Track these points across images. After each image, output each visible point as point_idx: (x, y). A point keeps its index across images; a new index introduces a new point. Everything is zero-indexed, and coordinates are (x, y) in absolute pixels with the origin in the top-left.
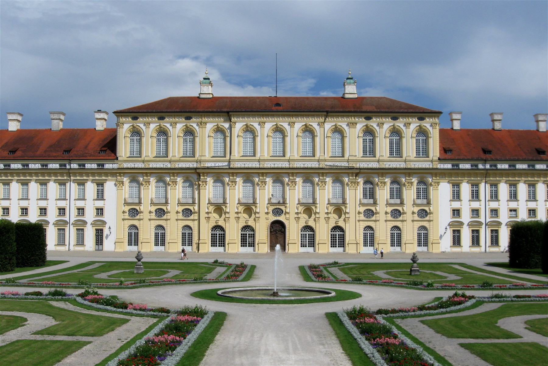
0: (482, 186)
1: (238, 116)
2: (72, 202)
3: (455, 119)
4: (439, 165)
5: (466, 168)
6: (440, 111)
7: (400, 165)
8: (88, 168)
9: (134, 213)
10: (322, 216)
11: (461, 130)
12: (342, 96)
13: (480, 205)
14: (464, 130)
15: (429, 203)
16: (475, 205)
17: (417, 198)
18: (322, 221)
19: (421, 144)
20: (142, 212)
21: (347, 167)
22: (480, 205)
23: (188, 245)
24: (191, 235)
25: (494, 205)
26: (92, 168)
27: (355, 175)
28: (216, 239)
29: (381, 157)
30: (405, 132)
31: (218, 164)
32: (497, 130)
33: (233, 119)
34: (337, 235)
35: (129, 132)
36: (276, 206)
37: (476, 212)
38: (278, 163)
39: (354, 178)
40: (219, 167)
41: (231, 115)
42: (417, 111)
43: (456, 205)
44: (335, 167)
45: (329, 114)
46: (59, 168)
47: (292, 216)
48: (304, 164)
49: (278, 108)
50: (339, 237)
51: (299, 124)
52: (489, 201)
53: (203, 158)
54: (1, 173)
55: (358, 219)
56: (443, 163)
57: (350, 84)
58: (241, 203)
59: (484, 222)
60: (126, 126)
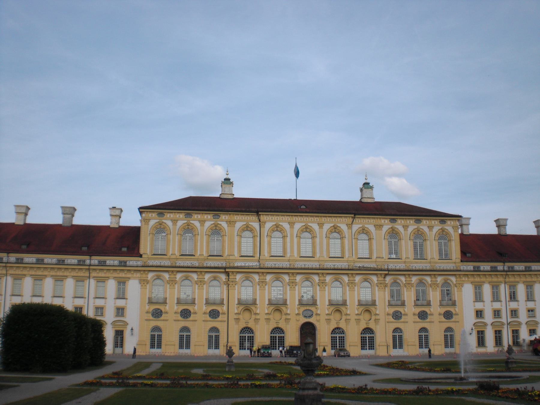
0: (502, 287)
2: (91, 300)
6: (460, 215)
9: (157, 314)
10: (353, 317)
13: (501, 306)
15: (454, 304)
16: (497, 305)
18: (353, 322)
19: (393, 246)
20: (406, 315)
22: (501, 306)
23: (215, 348)
24: (217, 337)
25: (513, 305)
27: (383, 276)
30: (428, 235)
31: (240, 264)
34: (338, 337)
35: (210, 230)
37: (497, 313)
39: (383, 279)
45: (356, 216)
46: (473, 270)
47: (323, 318)
50: (369, 340)
53: (231, 257)
55: (387, 320)
59: (505, 322)
60: (152, 223)
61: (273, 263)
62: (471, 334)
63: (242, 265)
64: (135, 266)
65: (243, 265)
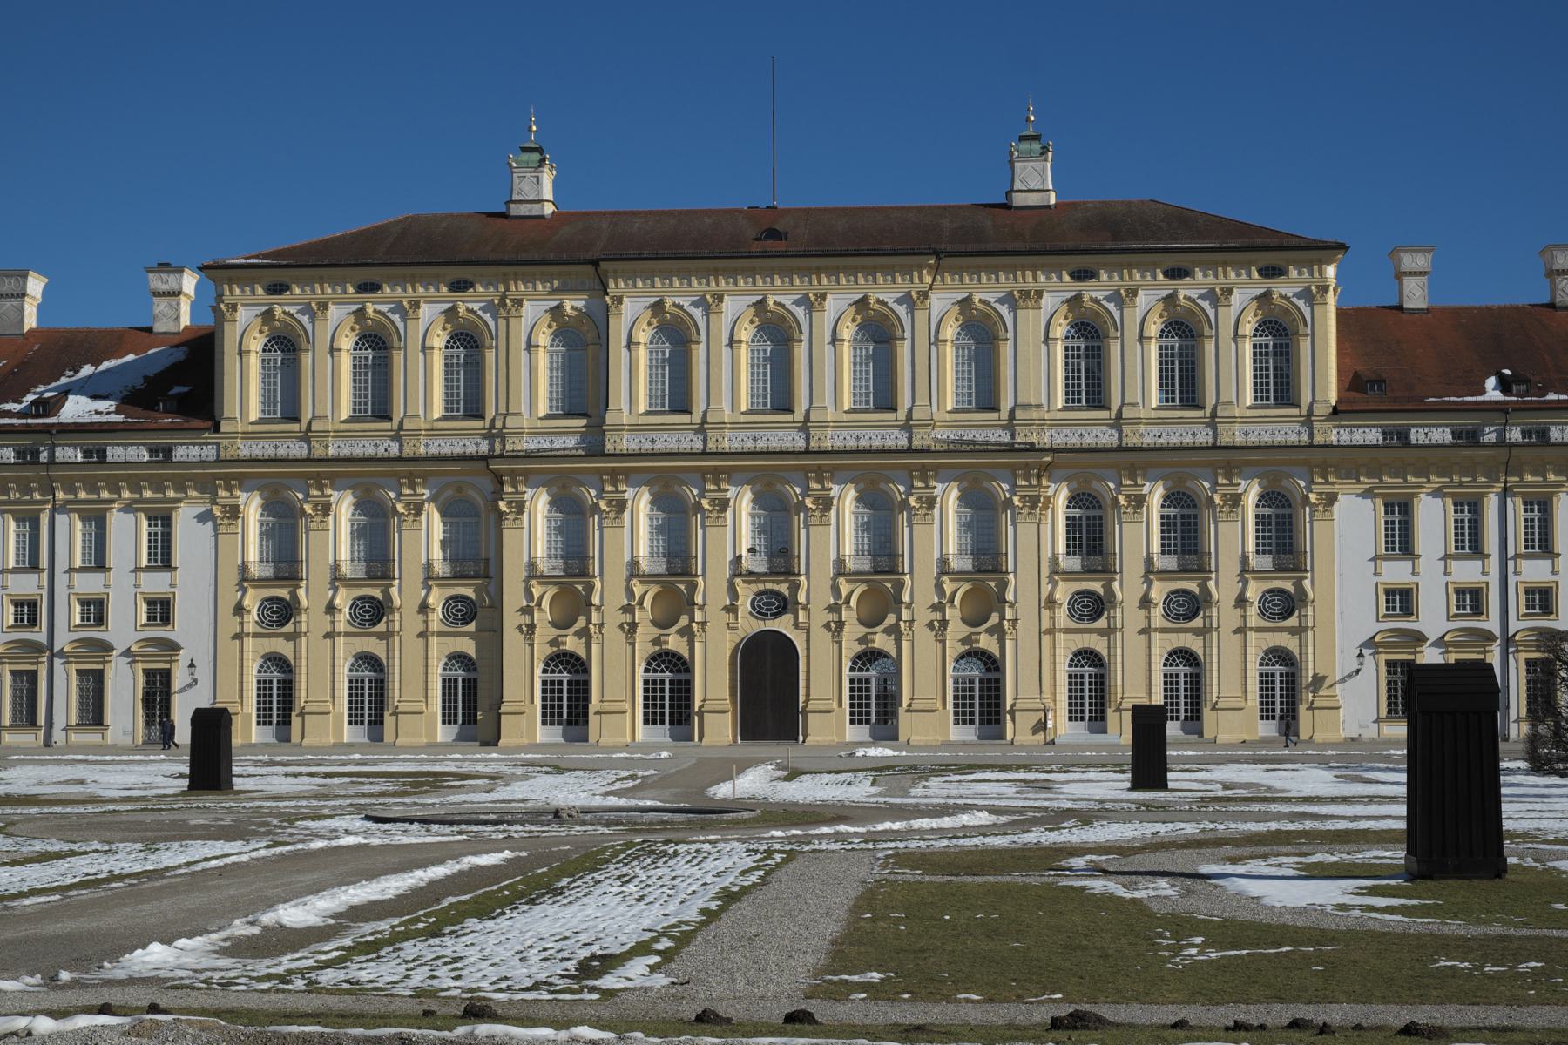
1: (630, 277)
3: (1410, 274)
4: (1335, 431)
5: (1434, 442)
7: (1194, 434)
8: (116, 459)
11: (1428, 310)
14: (1443, 310)
16: (1467, 572)
26: (129, 459)
28: (560, 699)
33: (612, 284)
36: (764, 582)
37: (1471, 599)
38: (768, 433)
39: (1035, 482)
40: (567, 452)
41: (606, 271)
42: (1258, 242)
43: (1397, 572)
47: (820, 617)
48: (858, 438)
49: (770, 245)
51: (838, 303)
52: (1516, 556)
56: (1347, 427)
58: (644, 576)
59: (1497, 632)
62: (1358, 671)
63: (541, 446)
64: (194, 460)
65: (545, 446)
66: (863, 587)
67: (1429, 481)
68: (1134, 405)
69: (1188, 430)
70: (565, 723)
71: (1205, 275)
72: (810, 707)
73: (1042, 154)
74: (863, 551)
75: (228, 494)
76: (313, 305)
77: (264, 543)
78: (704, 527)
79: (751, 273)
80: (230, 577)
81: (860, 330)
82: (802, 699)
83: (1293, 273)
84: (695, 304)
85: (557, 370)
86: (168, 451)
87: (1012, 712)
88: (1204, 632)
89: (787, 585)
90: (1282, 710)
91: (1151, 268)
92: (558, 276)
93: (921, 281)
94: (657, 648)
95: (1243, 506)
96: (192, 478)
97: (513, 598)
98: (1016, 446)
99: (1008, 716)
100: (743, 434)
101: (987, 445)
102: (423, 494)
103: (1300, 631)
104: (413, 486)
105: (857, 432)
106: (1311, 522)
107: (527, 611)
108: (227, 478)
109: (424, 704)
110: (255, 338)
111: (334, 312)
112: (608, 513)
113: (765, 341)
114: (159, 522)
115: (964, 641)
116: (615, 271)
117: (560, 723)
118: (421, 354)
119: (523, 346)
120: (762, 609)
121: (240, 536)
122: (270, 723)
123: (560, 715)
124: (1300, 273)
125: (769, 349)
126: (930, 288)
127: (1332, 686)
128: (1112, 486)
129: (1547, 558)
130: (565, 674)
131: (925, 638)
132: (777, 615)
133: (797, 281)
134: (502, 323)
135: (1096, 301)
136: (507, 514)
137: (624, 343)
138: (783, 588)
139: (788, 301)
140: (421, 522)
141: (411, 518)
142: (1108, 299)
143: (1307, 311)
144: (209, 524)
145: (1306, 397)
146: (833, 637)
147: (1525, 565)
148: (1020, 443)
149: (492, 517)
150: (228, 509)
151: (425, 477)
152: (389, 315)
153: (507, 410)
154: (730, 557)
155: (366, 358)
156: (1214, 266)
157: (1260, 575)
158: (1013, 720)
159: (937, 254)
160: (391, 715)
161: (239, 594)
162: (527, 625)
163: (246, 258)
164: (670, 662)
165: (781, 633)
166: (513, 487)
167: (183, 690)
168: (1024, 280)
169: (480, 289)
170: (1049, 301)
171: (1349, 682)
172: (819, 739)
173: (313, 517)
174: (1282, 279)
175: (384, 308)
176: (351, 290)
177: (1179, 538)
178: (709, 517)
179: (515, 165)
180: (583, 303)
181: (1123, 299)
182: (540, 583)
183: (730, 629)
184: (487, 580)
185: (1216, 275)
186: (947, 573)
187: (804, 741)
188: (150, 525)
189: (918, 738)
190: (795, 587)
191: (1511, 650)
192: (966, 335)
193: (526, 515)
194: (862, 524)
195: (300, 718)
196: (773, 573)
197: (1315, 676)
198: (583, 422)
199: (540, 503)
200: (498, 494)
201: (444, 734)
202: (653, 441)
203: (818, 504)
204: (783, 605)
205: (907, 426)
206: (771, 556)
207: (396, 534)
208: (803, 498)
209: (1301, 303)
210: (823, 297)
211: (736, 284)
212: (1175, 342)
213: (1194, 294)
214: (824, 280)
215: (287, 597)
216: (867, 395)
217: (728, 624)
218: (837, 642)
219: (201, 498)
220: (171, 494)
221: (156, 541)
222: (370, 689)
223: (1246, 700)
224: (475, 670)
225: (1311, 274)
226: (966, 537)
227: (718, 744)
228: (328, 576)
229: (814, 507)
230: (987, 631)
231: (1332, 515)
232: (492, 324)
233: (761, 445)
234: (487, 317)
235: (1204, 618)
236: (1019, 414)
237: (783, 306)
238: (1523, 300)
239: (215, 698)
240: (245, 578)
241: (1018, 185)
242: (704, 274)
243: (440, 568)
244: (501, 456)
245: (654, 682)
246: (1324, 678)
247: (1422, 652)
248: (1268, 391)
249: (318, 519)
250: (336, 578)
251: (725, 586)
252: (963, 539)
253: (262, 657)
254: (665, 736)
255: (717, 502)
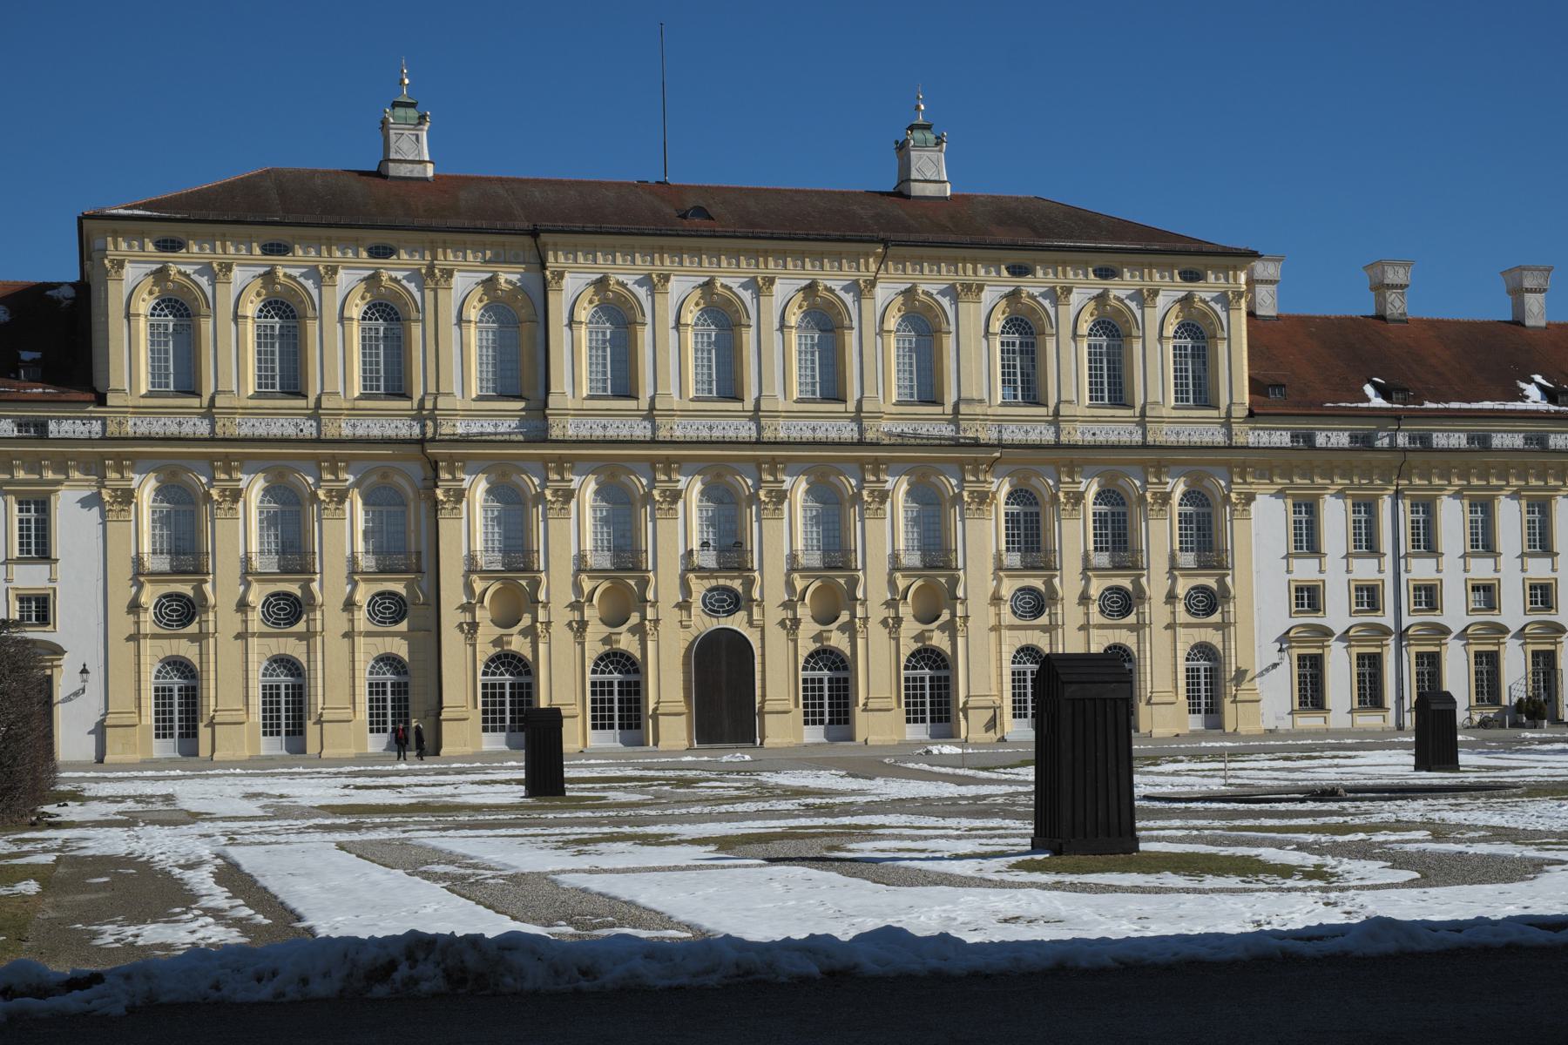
1: (572, 251)
11: (1278, 318)
12: (890, 187)
13: (1380, 571)
14: (1289, 318)
16: (1366, 570)
17: (1096, 549)
21: (951, 439)
25: (1421, 570)
29: (1066, 405)
32: (1395, 321)
33: (551, 258)
36: (717, 578)
37: (1368, 596)
38: (724, 422)
41: (545, 245)
43: (1306, 570)
44: (918, 441)
47: (774, 614)
48: (814, 429)
52: (1407, 555)
54: (11, 456)
56: (1267, 429)
57: (924, 145)
61: (584, 421)
62: (1275, 665)
64: (82, 437)
65: (489, 430)
66: (817, 583)
67: (1450, 484)
68: (1070, 402)
69: (1118, 429)
70: (507, 729)
71: (1132, 276)
72: (767, 708)
73: (937, 144)
74: (812, 546)
75: (118, 476)
76: (215, 265)
77: (157, 532)
78: (654, 520)
79: (697, 252)
80: (122, 572)
81: (805, 317)
82: (758, 699)
83: (1211, 277)
84: (639, 283)
85: (487, 348)
86: (41, 427)
87: (965, 710)
88: (1137, 628)
89: (740, 581)
90: (1206, 704)
91: (1084, 266)
92: (491, 246)
93: (867, 269)
94: (607, 648)
95: (1085, 504)
96: (76, 457)
97: (452, 594)
98: (962, 441)
99: (961, 714)
100: (697, 422)
101: (940, 439)
102: (347, 480)
103: (1223, 626)
104: (334, 471)
105: (813, 423)
106: (1231, 520)
107: (465, 608)
108: (119, 459)
109: (351, 711)
110: (143, 300)
111: (239, 275)
112: (553, 503)
113: (708, 325)
114: (33, 507)
115: (917, 638)
116: (555, 245)
117: (502, 729)
118: (338, 325)
119: (454, 321)
120: (714, 606)
121: (133, 523)
122: (172, 735)
123: (503, 720)
124: (1217, 278)
125: (713, 334)
126: (876, 278)
127: (1253, 679)
128: (1051, 482)
129: (1375, 558)
130: (507, 676)
131: (878, 634)
132: (730, 613)
133: (743, 263)
134: (429, 295)
135: (1032, 297)
136: (445, 503)
137: (565, 321)
138: (737, 585)
139: (734, 283)
140: (344, 511)
141: (332, 506)
142: (1043, 295)
143: (1223, 316)
144: (96, 510)
145: (1224, 400)
146: (788, 635)
147: (1414, 562)
148: (965, 438)
149: (424, 507)
150: (119, 493)
151: (348, 459)
152: (302, 280)
153: (438, 389)
154: (681, 551)
155: (272, 328)
156: (1140, 267)
157: (1188, 572)
158: (966, 718)
159: (885, 243)
160: (315, 723)
161: (134, 590)
162: (468, 624)
163: (126, 208)
164: (618, 662)
165: (736, 632)
166: (450, 473)
167: (67, 699)
168: (965, 272)
169: (404, 256)
170: (989, 296)
171: (1267, 676)
172: (777, 741)
173: (220, 503)
174: (1201, 283)
175: (295, 272)
176: (257, 251)
177: (1110, 536)
178: (659, 509)
179: (392, 121)
180: (519, 276)
181: (1058, 296)
182: (481, 578)
183: (683, 627)
184: (420, 575)
185: (1142, 277)
186: (898, 570)
187: (761, 744)
188: (21, 510)
189: (875, 738)
190: (749, 583)
191: (1404, 643)
192: (906, 326)
193: (464, 504)
194: (811, 519)
195: (209, 729)
196: (724, 568)
197: (1238, 669)
198: (521, 405)
199: (478, 489)
200: (435, 481)
201: (377, 743)
202: (605, 427)
203: (771, 497)
204: (732, 602)
205: (858, 417)
206: (721, 551)
207: (316, 524)
208: (757, 491)
209: (1218, 307)
210: (771, 281)
211: (681, 263)
212: (1103, 341)
213: (1122, 294)
214: (771, 264)
215: (191, 593)
216: (814, 384)
217: (681, 622)
218: (792, 640)
219: (87, 480)
220: (49, 475)
221: (29, 529)
222: (287, 695)
223: (1177, 694)
224: (406, 673)
225: (1227, 279)
226: (913, 532)
227: (675, 748)
228: (238, 571)
229: (767, 500)
230: (939, 628)
231: (1250, 515)
232: (417, 296)
233: (717, 434)
234: (412, 287)
235: (1137, 614)
236: (963, 409)
237: (730, 289)
238: (1356, 312)
239: (107, 707)
240: (139, 574)
241: (914, 175)
242: (649, 252)
243: (366, 562)
244: (433, 440)
245: (602, 684)
246: (1246, 671)
247: (1504, 643)
248: (1102, 391)
249: (225, 506)
250: (247, 574)
251: (677, 581)
252: (910, 534)
253: (161, 661)
254: (615, 741)
255: (668, 493)
